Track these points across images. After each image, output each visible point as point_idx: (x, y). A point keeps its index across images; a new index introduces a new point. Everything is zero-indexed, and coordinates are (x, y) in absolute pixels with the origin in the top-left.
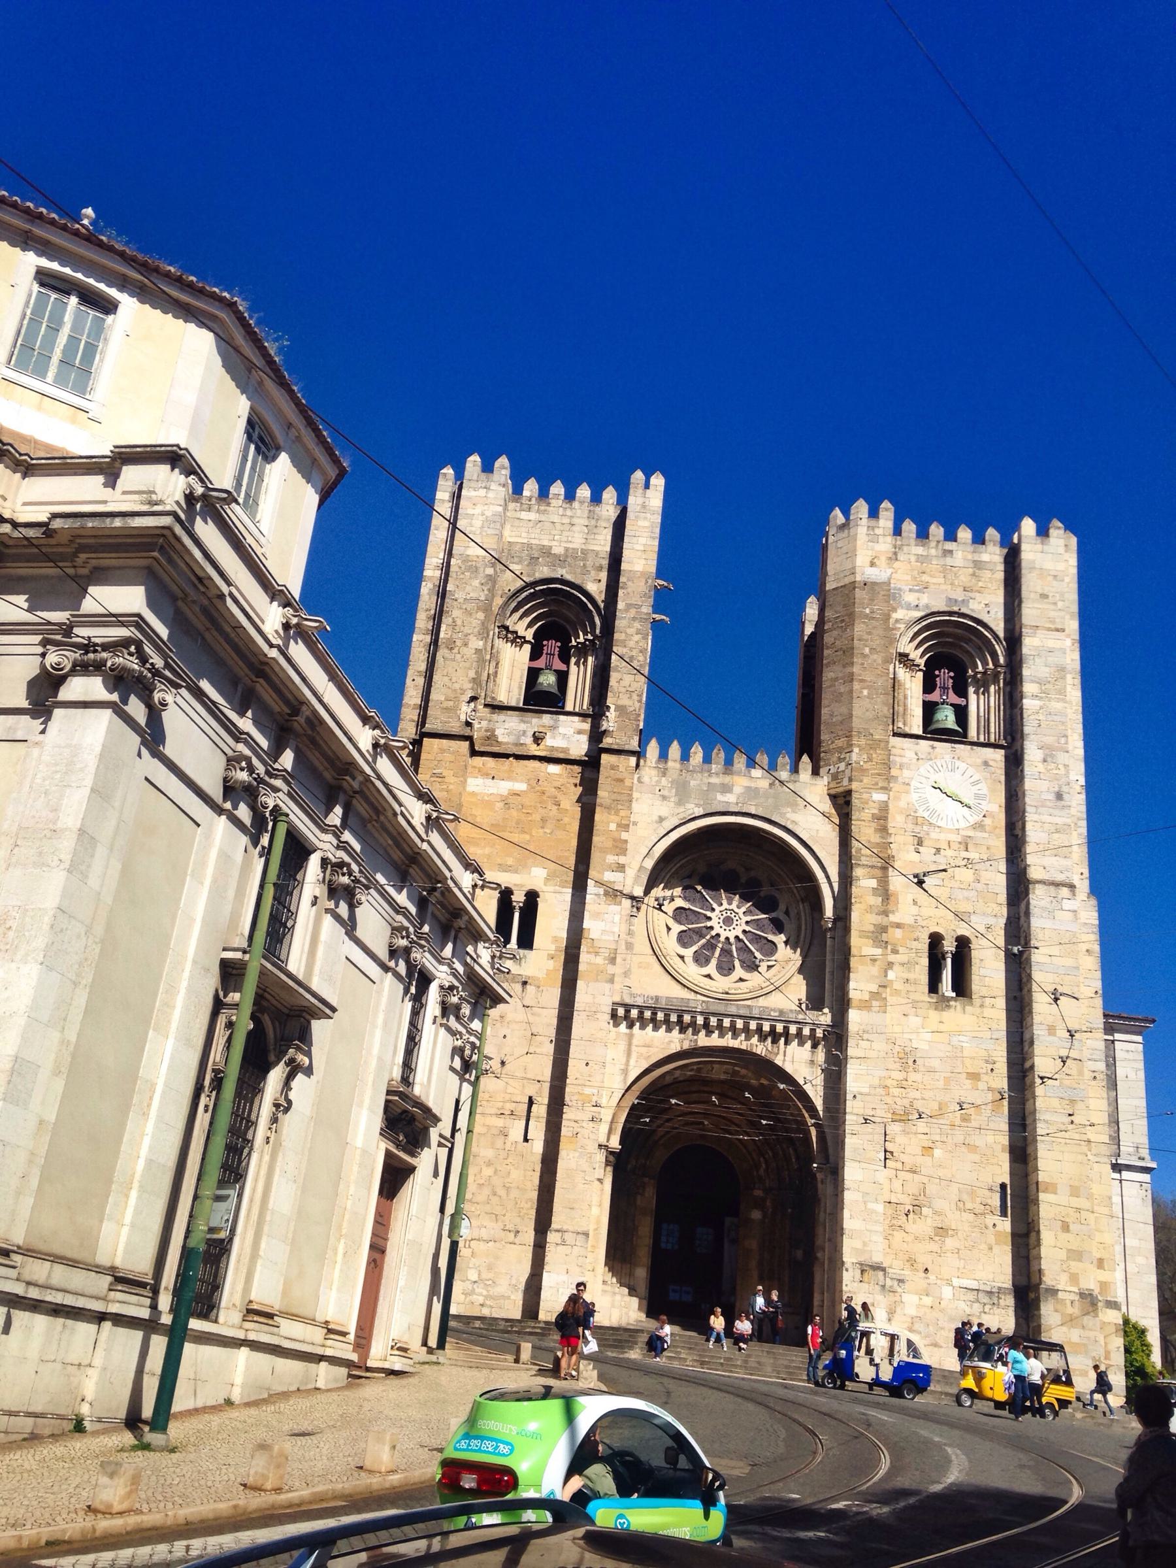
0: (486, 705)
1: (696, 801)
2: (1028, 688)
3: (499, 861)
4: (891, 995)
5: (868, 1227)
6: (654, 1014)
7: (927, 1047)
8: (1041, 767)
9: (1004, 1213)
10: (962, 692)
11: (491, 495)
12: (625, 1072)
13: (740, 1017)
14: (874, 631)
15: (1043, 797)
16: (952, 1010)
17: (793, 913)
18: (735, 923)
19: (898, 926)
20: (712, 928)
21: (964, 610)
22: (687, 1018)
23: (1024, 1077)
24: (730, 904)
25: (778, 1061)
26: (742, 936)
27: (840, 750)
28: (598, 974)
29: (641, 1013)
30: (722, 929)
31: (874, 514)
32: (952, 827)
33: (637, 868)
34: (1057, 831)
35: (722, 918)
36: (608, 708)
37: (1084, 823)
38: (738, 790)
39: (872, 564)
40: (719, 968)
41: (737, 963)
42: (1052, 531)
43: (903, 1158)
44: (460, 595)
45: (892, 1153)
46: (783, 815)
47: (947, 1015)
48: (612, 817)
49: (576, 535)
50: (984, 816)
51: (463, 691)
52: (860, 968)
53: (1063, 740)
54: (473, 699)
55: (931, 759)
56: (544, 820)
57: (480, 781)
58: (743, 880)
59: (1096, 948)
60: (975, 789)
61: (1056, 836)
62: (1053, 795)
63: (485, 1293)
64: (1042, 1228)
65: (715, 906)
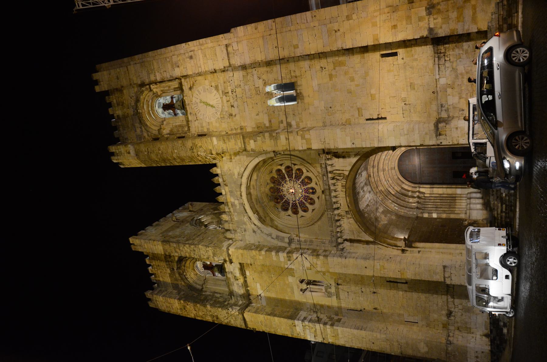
0: (232, 298)
4: (302, 122)
7: (323, 102)
8: (181, 68)
9: (395, 54)
12: (368, 243)
13: (330, 195)
16: (302, 91)
17: (281, 163)
19: (270, 121)
22: (337, 218)
25: (347, 173)
31: (113, 154)
34: (206, 56)
37: (201, 40)
39: (129, 153)
40: (313, 193)
41: (309, 186)
42: (95, 78)
47: (305, 94)
49: (161, 264)
50: (212, 86)
53: (168, 60)
55: (196, 114)
58: (273, 186)
59: (253, 25)
61: (207, 55)
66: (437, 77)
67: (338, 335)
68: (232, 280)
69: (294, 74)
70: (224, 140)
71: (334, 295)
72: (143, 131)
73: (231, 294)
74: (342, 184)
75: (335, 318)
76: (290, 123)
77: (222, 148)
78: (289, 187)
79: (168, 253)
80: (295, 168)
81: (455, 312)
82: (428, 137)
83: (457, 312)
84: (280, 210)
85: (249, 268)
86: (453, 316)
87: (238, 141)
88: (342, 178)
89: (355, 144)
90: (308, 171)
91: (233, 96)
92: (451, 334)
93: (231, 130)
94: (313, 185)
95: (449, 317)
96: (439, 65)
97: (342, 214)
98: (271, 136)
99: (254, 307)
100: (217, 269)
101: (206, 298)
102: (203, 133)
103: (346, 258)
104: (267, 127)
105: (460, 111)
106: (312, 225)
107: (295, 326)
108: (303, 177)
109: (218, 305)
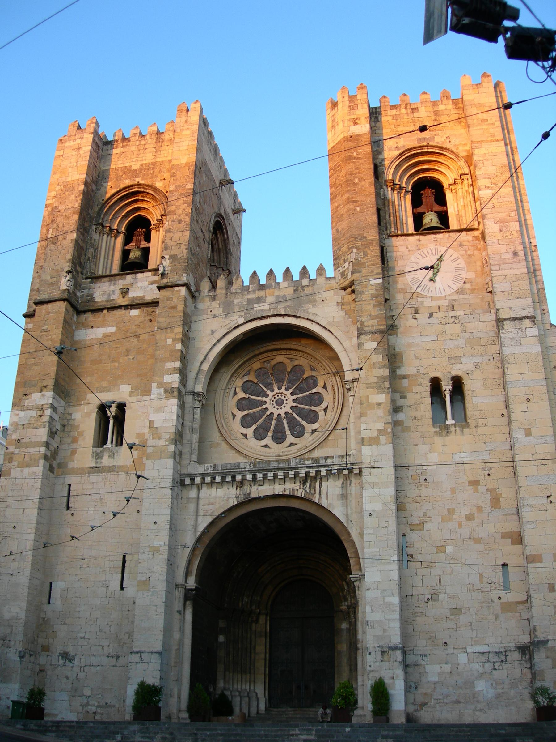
0: (87, 278)
1: (239, 314)
2: (482, 182)
3: (97, 385)
4: (403, 431)
5: (387, 617)
6: (214, 479)
8: (499, 236)
9: (506, 587)
10: (441, 199)
11: (84, 141)
12: (195, 527)
14: (362, 167)
15: (503, 257)
16: (453, 433)
18: (285, 402)
19: (405, 377)
20: (267, 409)
21: (431, 143)
22: (239, 477)
23: (515, 473)
24: (280, 388)
26: (290, 411)
27: (344, 254)
28: (159, 454)
29: (203, 479)
30: (276, 409)
32: (440, 295)
33: (196, 370)
34: (517, 280)
35: (275, 400)
36: (163, 258)
38: (270, 299)
39: (355, 123)
41: (288, 432)
43: (420, 558)
44: (62, 208)
45: (412, 556)
46: (306, 311)
47: (448, 439)
48: (169, 335)
49: (148, 155)
50: (464, 283)
51: (62, 269)
52: (369, 412)
54: (68, 272)
56: (128, 351)
57: (83, 331)
60: (455, 265)
61: (516, 283)
62: (511, 253)
63: (96, 704)
64: (532, 592)
65: (269, 392)
66: (469, 650)
67: (27, 466)
68: (121, 283)
69: (480, 424)
70: (376, 296)
71: (96, 463)
72: (389, 151)
73: (96, 278)
74: (297, 490)
75: (54, 461)
76: (402, 411)
77: (363, 292)
78: (286, 398)
79: (174, 173)
80: (320, 411)
81: (72, 667)
82: (380, 633)
83: (71, 670)
84: (246, 378)
85: (145, 316)
86: (65, 663)
87: (375, 321)
88: (308, 491)
89: (369, 516)
90: (314, 431)
91: (448, 317)
92: (32, 659)
93: (390, 309)
94: (290, 439)
95: (62, 657)
96: (489, 652)
97: (246, 487)
98: (382, 379)
99: (71, 319)
100: (137, 256)
101: (86, 232)
102: (385, 259)
103: (172, 489)
104: (395, 371)
105: (415, 684)
106: (221, 433)
107: (41, 391)
108: (303, 423)
109: (76, 253)
